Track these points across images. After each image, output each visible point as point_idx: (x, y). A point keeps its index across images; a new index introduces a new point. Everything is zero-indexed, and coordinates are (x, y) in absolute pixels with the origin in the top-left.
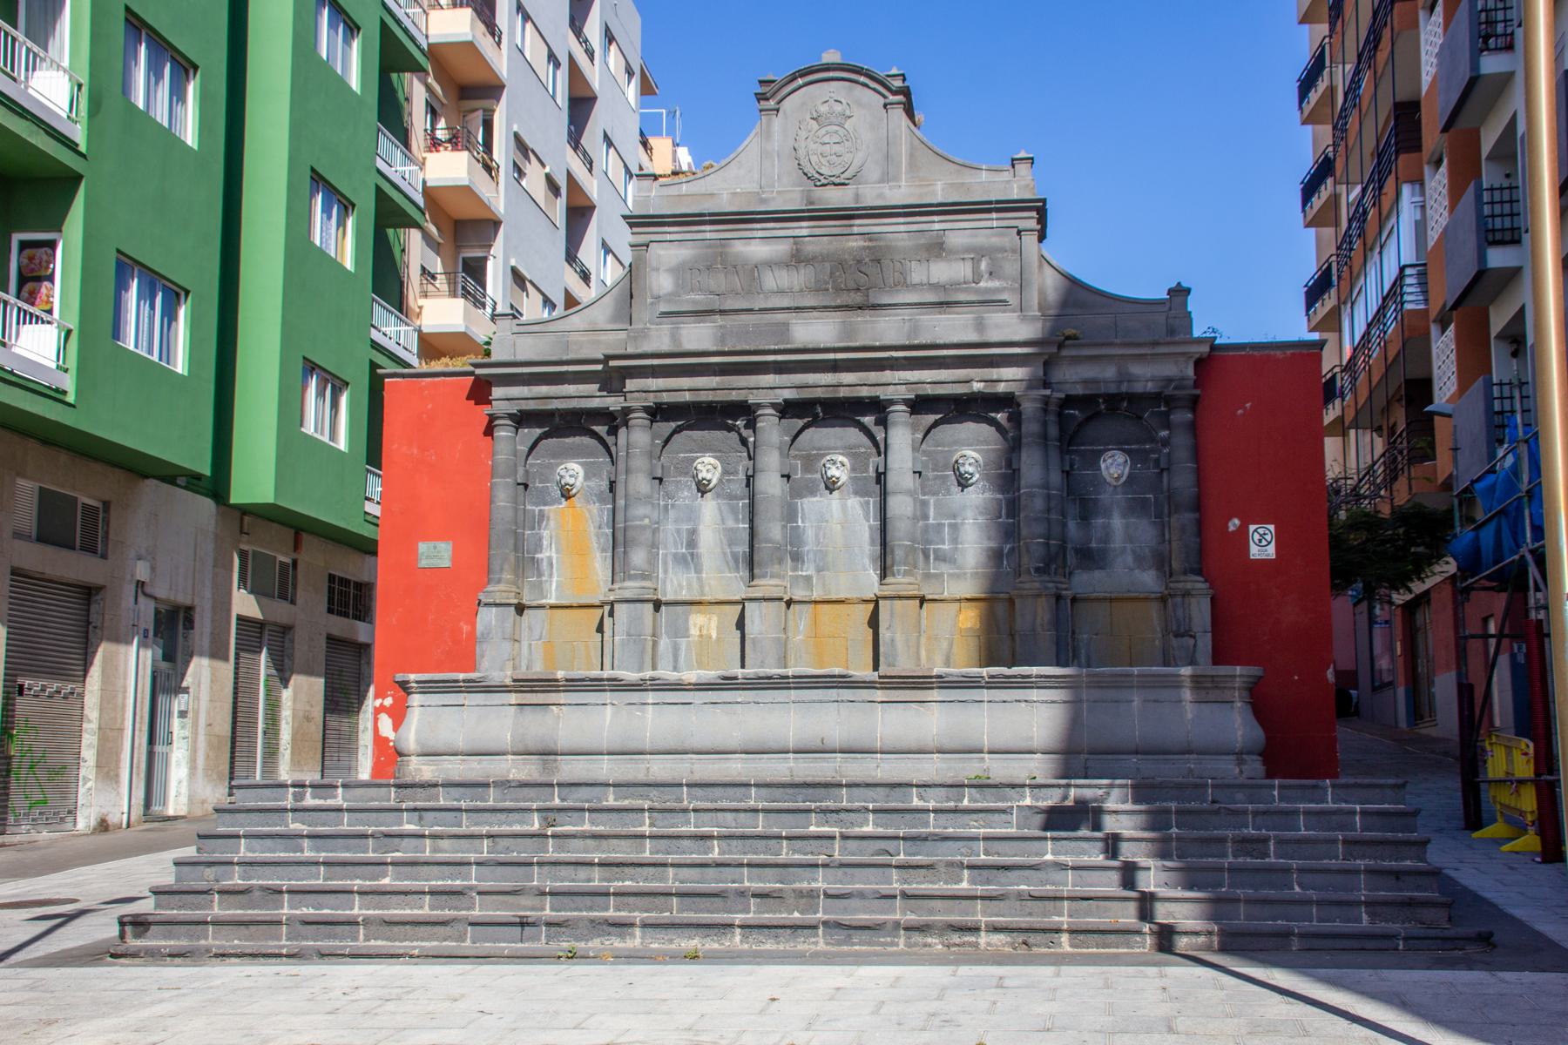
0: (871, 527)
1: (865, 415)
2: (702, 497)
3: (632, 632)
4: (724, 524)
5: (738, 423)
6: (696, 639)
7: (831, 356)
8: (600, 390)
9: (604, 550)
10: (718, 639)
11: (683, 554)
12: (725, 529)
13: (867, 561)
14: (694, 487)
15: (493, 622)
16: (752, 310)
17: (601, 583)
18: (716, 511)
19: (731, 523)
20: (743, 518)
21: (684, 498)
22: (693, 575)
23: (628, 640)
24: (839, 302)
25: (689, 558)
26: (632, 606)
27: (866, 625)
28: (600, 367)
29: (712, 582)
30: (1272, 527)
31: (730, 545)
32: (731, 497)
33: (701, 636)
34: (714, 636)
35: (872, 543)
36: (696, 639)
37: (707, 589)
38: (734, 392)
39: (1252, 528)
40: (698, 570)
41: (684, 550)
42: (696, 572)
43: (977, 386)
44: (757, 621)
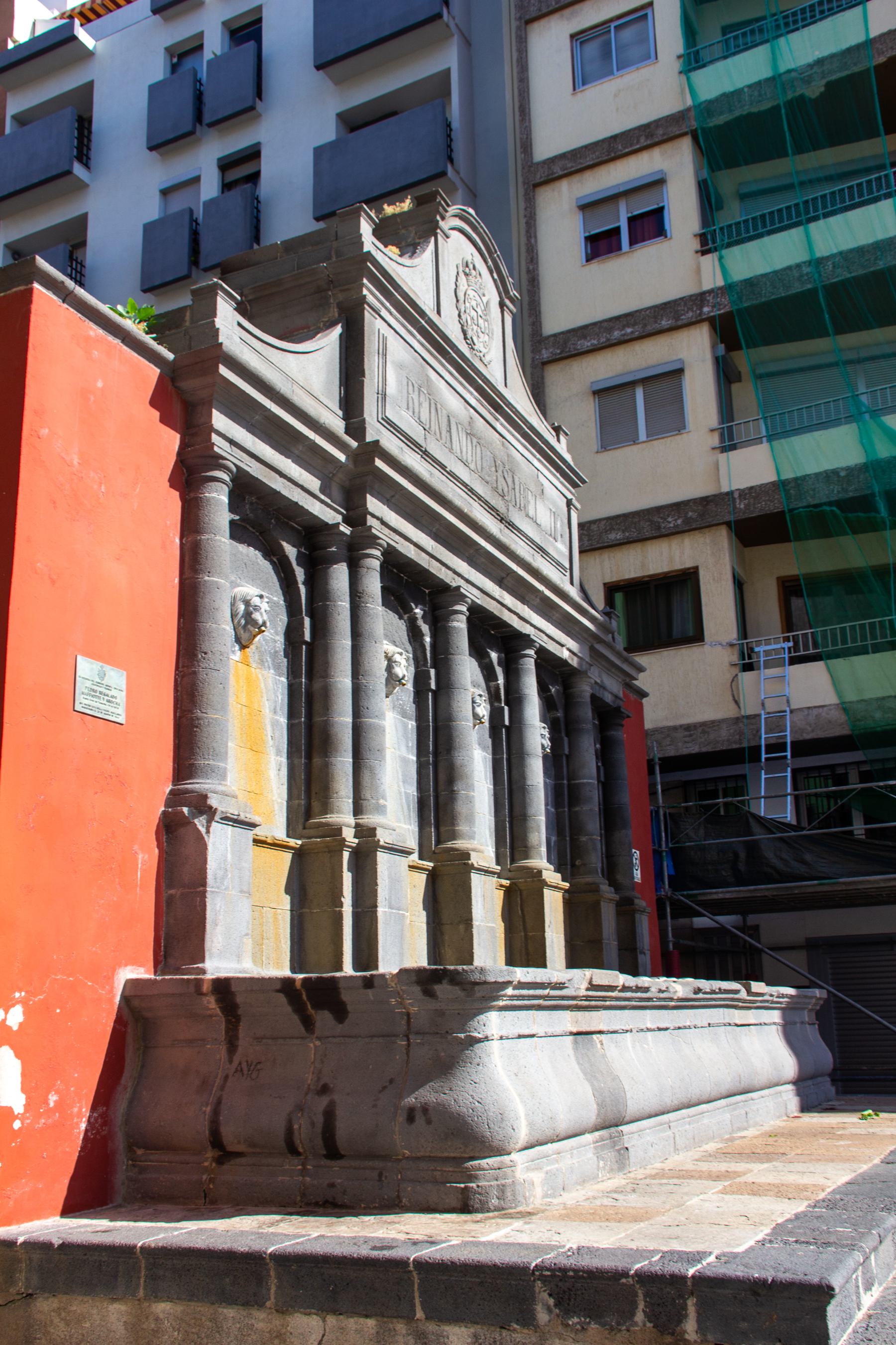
9: (278, 753)
15: (229, 856)
16: (443, 467)
17: (276, 807)
18: (394, 728)
24: (493, 502)
28: (342, 457)
38: (444, 569)
43: (565, 654)
44: (480, 900)
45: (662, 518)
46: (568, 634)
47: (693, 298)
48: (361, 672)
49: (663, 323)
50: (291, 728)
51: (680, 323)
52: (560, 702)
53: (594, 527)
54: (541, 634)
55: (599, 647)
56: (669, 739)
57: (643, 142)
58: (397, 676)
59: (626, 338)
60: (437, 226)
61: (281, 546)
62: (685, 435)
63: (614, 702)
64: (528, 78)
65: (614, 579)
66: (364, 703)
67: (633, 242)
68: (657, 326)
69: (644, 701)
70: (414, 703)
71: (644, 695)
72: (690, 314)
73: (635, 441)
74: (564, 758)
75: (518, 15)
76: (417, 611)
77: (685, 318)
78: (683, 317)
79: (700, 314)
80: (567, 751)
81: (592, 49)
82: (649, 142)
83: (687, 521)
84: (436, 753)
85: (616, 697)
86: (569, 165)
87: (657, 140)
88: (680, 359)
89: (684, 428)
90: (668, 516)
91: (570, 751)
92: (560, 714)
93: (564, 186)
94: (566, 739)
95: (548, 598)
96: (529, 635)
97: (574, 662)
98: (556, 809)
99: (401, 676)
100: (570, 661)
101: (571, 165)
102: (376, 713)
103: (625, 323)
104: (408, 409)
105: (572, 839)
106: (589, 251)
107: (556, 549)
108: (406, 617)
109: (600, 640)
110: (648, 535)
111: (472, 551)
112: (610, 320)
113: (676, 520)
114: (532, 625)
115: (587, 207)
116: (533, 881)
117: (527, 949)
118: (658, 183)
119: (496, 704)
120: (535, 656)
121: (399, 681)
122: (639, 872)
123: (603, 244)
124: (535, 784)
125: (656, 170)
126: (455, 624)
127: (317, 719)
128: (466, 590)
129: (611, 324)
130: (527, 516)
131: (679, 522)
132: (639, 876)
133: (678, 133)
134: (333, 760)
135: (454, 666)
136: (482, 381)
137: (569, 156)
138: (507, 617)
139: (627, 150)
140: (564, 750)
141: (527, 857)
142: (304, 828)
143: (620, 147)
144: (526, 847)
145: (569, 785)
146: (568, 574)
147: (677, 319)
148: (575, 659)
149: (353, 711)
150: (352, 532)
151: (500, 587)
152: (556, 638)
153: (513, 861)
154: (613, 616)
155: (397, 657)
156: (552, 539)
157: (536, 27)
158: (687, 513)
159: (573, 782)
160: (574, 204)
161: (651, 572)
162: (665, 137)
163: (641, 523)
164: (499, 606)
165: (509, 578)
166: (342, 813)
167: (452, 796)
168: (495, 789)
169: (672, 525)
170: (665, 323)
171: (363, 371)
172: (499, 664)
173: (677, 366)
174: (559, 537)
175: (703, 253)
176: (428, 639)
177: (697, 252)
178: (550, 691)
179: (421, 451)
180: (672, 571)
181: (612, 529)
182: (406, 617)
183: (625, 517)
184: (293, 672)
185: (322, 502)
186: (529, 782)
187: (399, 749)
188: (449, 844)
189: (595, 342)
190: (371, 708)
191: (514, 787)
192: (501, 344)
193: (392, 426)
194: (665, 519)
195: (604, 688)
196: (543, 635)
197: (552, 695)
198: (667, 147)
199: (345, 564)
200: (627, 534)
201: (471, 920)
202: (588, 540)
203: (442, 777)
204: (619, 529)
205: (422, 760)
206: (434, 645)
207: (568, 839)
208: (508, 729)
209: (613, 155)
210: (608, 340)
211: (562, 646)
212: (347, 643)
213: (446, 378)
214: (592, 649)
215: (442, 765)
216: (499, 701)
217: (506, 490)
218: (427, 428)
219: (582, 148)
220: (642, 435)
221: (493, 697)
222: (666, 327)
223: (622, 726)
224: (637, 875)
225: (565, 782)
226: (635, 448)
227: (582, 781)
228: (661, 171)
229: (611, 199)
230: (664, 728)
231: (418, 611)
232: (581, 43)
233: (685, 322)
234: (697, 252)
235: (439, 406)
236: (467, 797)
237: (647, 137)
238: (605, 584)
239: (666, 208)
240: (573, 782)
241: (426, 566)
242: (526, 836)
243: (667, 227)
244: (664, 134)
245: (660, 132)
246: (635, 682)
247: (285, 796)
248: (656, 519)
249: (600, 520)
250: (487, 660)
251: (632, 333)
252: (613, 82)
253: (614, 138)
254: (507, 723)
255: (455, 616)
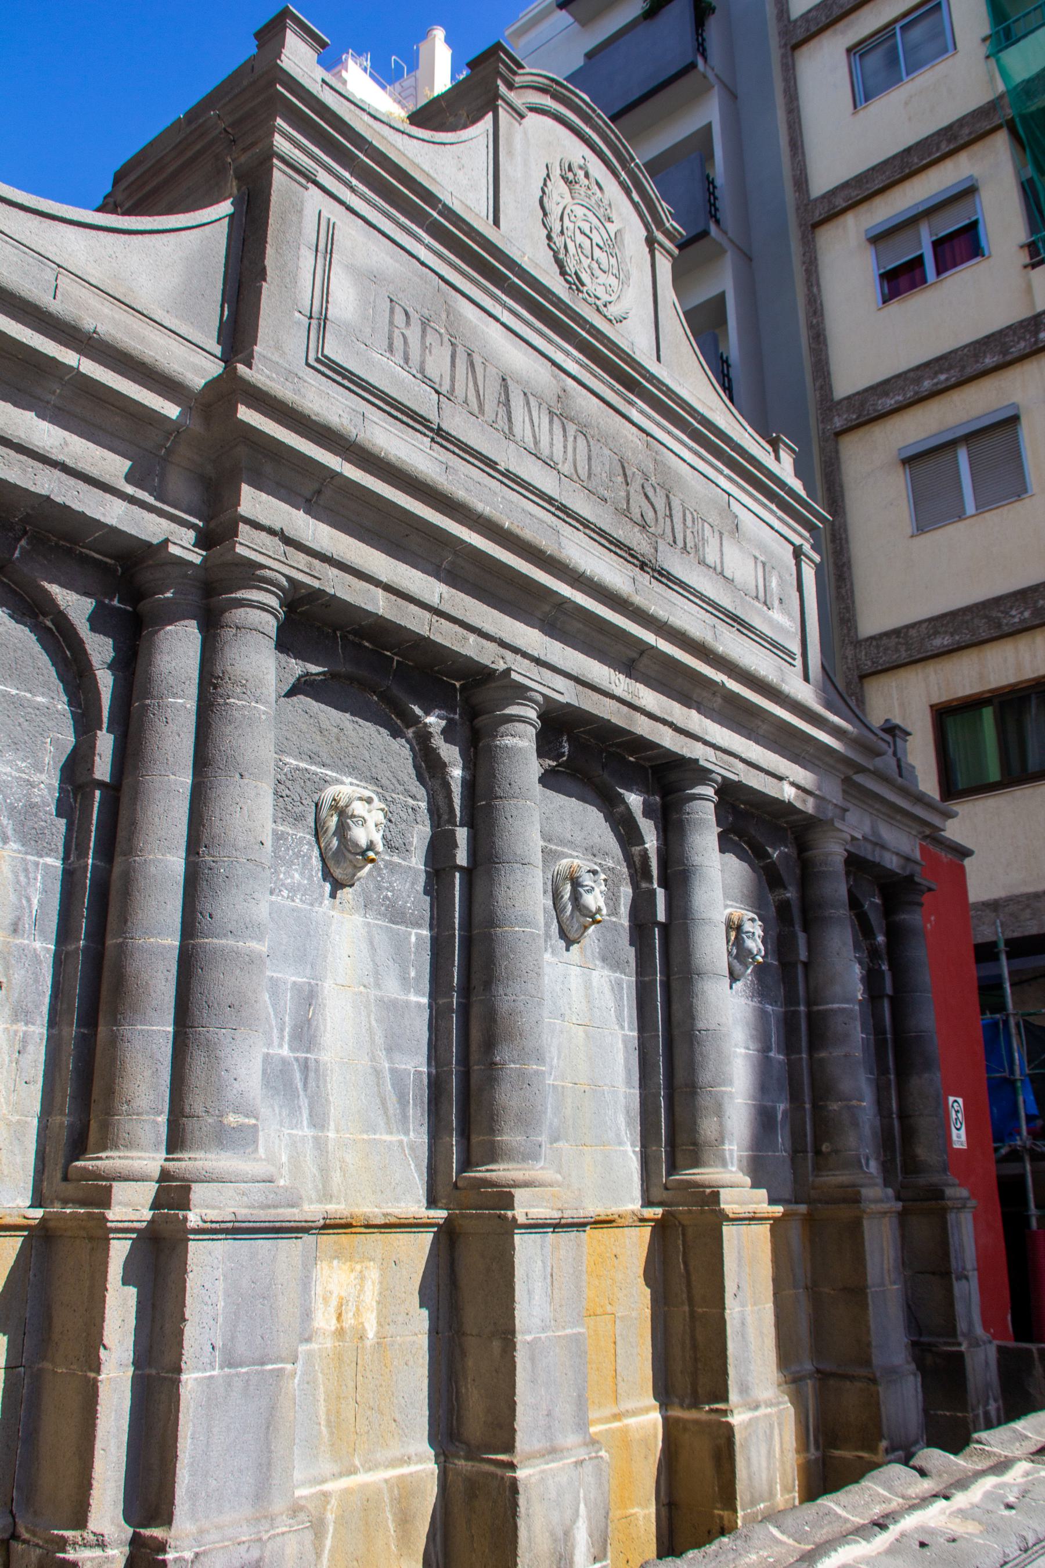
0: (625, 1040)
1: (631, 791)
2: (333, 895)
3: (241, 1349)
4: (378, 985)
5: (431, 719)
6: (329, 1343)
7: (649, 637)
8: (129, 478)
10: (381, 1336)
11: (284, 1061)
12: (380, 1000)
13: (621, 1119)
14: (316, 863)
16: (491, 464)
18: (364, 946)
19: (392, 989)
20: (418, 978)
21: (293, 889)
22: (308, 1132)
23: (228, 1382)
24: (619, 534)
25: (298, 1076)
26: (242, 1247)
27: (641, 1281)
28: (172, 411)
29: (349, 1158)
30: (960, 1100)
31: (389, 1050)
32: (396, 915)
33: (340, 1333)
34: (371, 1334)
35: (629, 1083)
36: (329, 1343)
37: (337, 1177)
38: (472, 638)
39: (951, 1099)
40: (318, 1121)
41: (285, 1051)
42: (313, 1125)
43: (789, 793)
44: (539, 1288)
45: (1002, 612)
46: (795, 758)
47: (1025, 323)
48: (205, 840)
49: (987, 361)
50: (60, 961)
51: (1009, 358)
52: (790, 875)
53: (913, 632)
54: (731, 759)
55: (859, 778)
56: (1028, 911)
57: (945, 148)
58: (357, 845)
59: (940, 387)
60: (497, 96)
61: (47, 594)
62: (1027, 501)
63: (904, 868)
64: (798, 107)
65: (944, 699)
66: (205, 905)
67: (940, 271)
68: (979, 367)
69: (967, 862)
70: (426, 892)
71: (966, 853)
72: (1022, 344)
73: (961, 516)
74: (800, 969)
75: (783, 42)
76: (431, 719)
77: (1015, 351)
78: (1013, 350)
79: (1036, 342)
80: (803, 956)
81: (874, 59)
82: (952, 146)
83: (1037, 612)
84: (466, 989)
85: (908, 859)
86: (854, 194)
87: (962, 142)
88: (1013, 404)
89: (1025, 491)
90: (1011, 608)
91: (810, 955)
92: (791, 894)
93: (850, 219)
94: (802, 938)
95: (737, 696)
96: (697, 760)
97: (809, 806)
98: (787, 1055)
99: (363, 843)
100: (799, 805)
101: (856, 194)
102: (230, 927)
103: (937, 368)
104: (391, 349)
105: (815, 1106)
106: (886, 290)
107: (770, 621)
108: (410, 733)
109: (861, 769)
110: (985, 635)
111: (547, 608)
112: (918, 368)
113: (1022, 613)
114: (706, 743)
115: (878, 239)
116: (702, 1212)
117: (693, 1338)
118: (968, 192)
119: (644, 885)
120: (716, 798)
121: (363, 853)
122: (963, 1132)
123: (903, 281)
124: (711, 1027)
125: (964, 177)
126: (508, 741)
127: (111, 942)
128: (523, 672)
129: (919, 373)
130: (702, 562)
131: (1027, 614)
132: (964, 1138)
133: (988, 127)
134: (126, 1030)
135: (502, 820)
136: (588, 332)
137: (853, 183)
138: (643, 727)
139: (924, 162)
140: (798, 954)
141: (696, 1162)
142: (65, 1178)
143: (916, 160)
144: (695, 1143)
145: (810, 1015)
146: (798, 662)
147: (1005, 353)
148: (811, 801)
149: (183, 923)
150: (205, 559)
151: (629, 676)
152: (765, 766)
153: (672, 1169)
154: (897, 732)
155: (359, 808)
156: (760, 606)
157: (805, 50)
158: (1037, 602)
159: (815, 1008)
160: (863, 238)
161: (993, 685)
162: (973, 136)
163: (976, 621)
164: (625, 709)
165: (645, 660)
166: (138, 1147)
167: (492, 1072)
168: (641, 1039)
169: (1016, 620)
170: (989, 361)
171: (264, 268)
172: (647, 813)
173: (1010, 413)
174: (776, 603)
175: (1034, 266)
176: (457, 773)
177: (1025, 267)
178: (769, 856)
179: (431, 430)
180: (1021, 682)
181: (936, 633)
182: (410, 733)
183: (953, 615)
184: (73, 848)
185: (132, 500)
186: (701, 1025)
187: (378, 985)
188: (480, 1173)
189: (900, 398)
190: (218, 915)
191: (676, 1032)
192: (651, 298)
193: (344, 377)
194: (1007, 613)
195: (883, 847)
196: (737, 761)
197: (773, 863)
198: (977, 148)
199: (194, 623)
200: (957, 638)
201: (512, 1332)
202: (906, 651)
203: (476, 1035)
204: (946, 632)
205: (441, 1002)
206: (470, 786)
207: (808, 1106)
208: (665, 928)
209: (907, 171)
210: (916, 393)
211: (780, 778)
212: (185, 780)
213: (504, 319)
214: (847, 781)
215: (476, 1011)
216: (649, 878)
217: (650, 515)
218: (445, 388)
219: (868, 170)
220: (970, 508)
221: (638, 871)
222: (991, 366)
223: (920, 905)
224: (959, 1138)
225: (802, 1008)
226: (961, 525)
227: (830, 1006)
228: (971, 177)
229: (910, 222)
230: (1022, 895)
231: (434, 721)
232: (861, 56)
233: (1015, 355)
234: (1025, 267)
235: (477, 360)
236: (521, 1074)
237: (949, 141)
238: (931, 706)
239: (981, 221)
240: (815, 1008)
241: (424, 631)
242: (695, 1123)
243: (983, 243)
244: (970, 133)
245: (966, 131)
246: (942, 833)
247: (36, 1106)
248: (995, 614)
249: (920, 623)
250: (622, 808)
251: (947, 379)
252: (902, 89)
253: (908, 151)
254: (661, 917)
255: (509, 726)
